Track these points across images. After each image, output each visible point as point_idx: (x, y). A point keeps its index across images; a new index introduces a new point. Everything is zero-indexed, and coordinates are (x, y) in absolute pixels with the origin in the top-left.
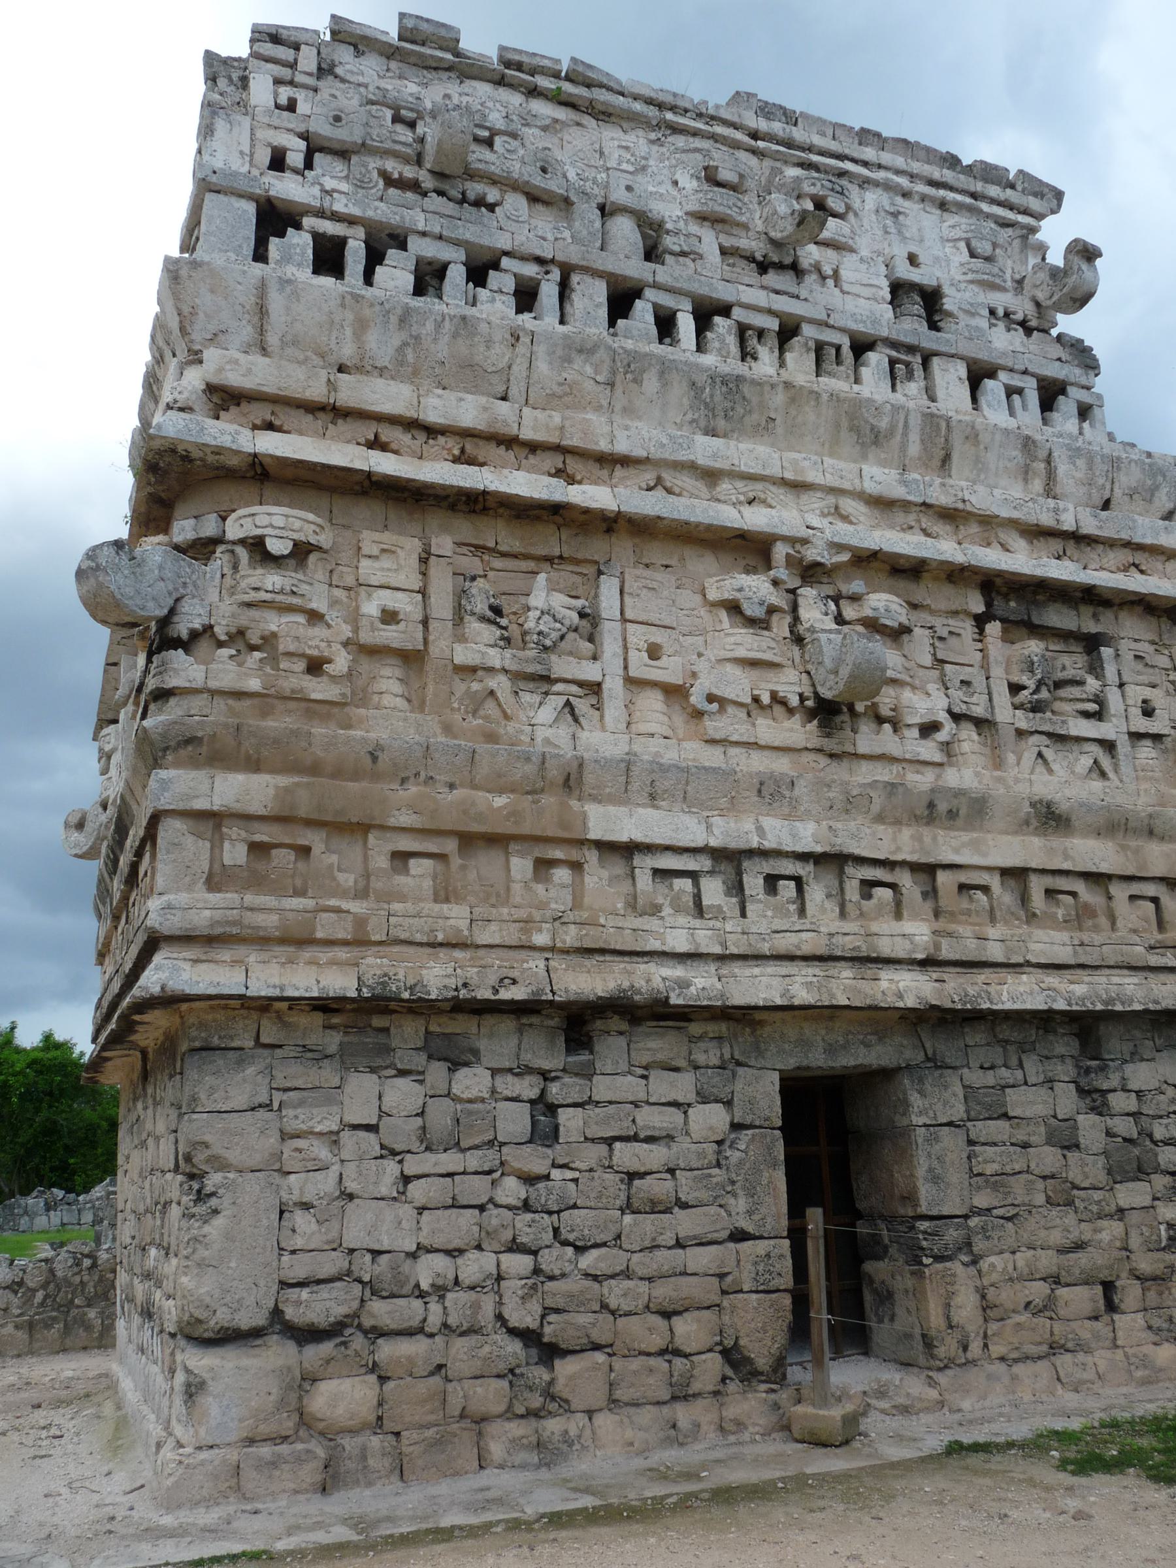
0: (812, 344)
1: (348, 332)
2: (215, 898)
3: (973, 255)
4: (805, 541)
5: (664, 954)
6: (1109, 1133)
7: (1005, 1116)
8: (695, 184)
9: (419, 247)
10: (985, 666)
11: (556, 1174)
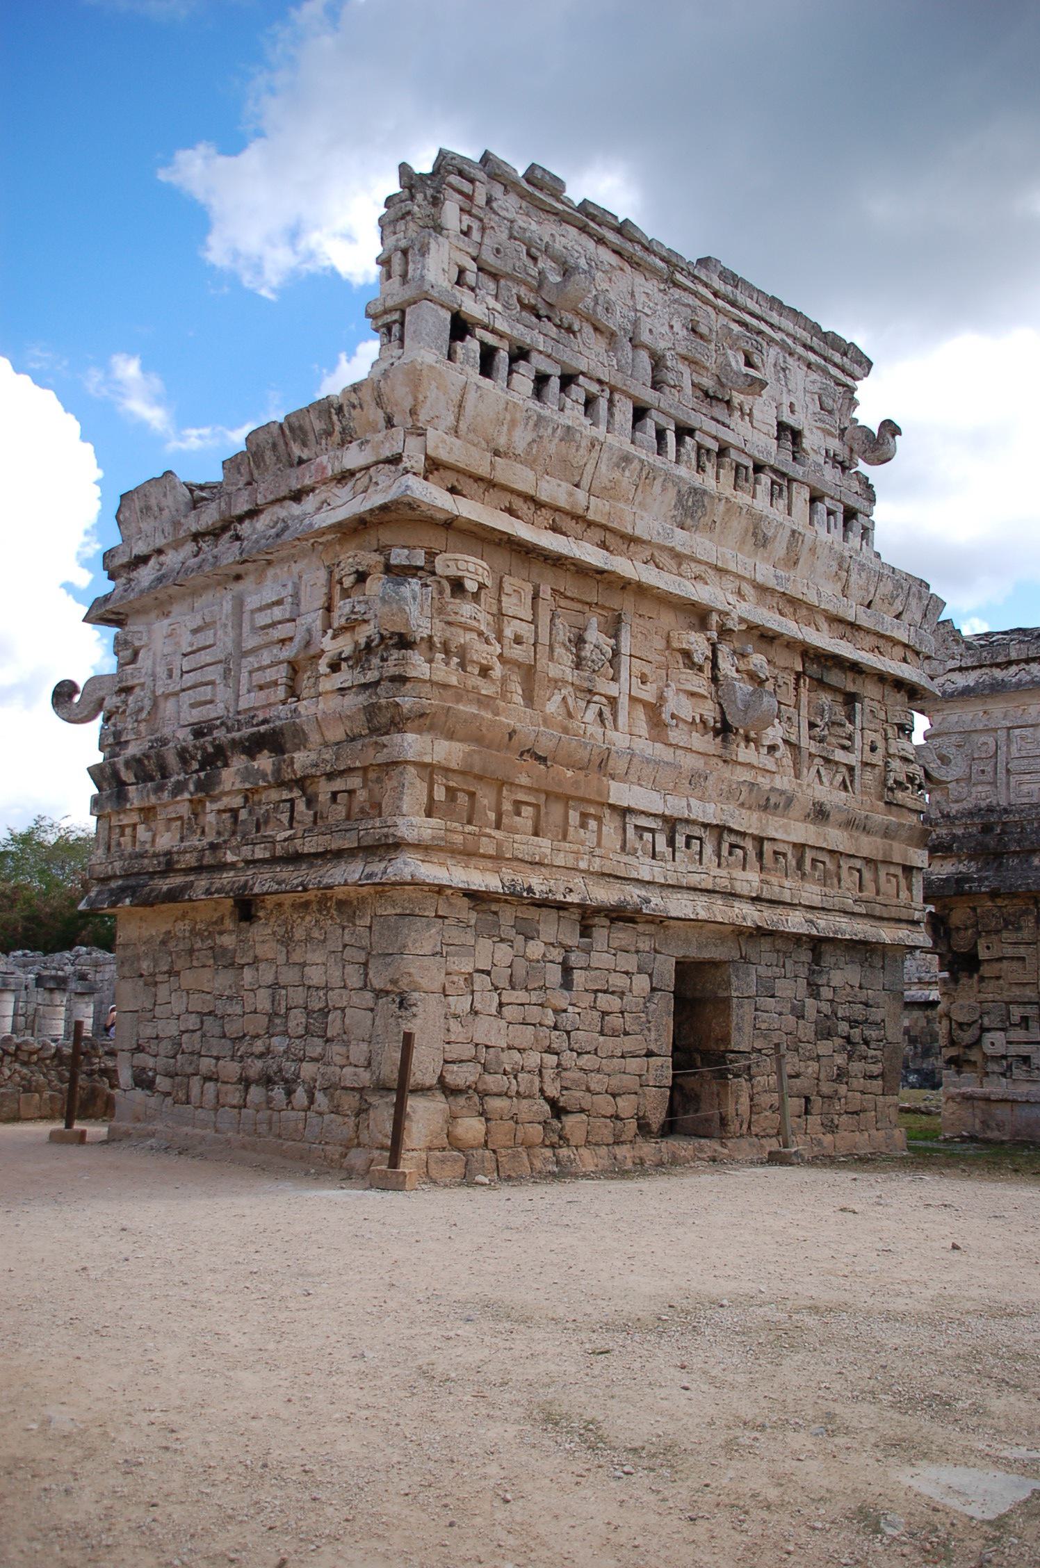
1: (505, 428)
2: (433, 821)
4: (727, 614)
5: (637, 880)
7: (773, 996)
8: (685, 331)
9: (539, 363)
10: (797, 706)
11: (570, 1009)
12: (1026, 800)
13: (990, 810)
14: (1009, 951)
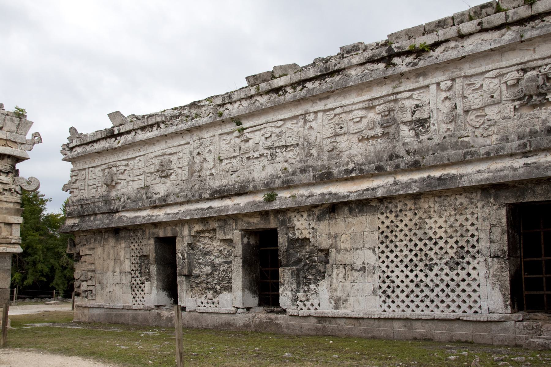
12: (92, 195)
13: (83, 200)
14: (88, 252)
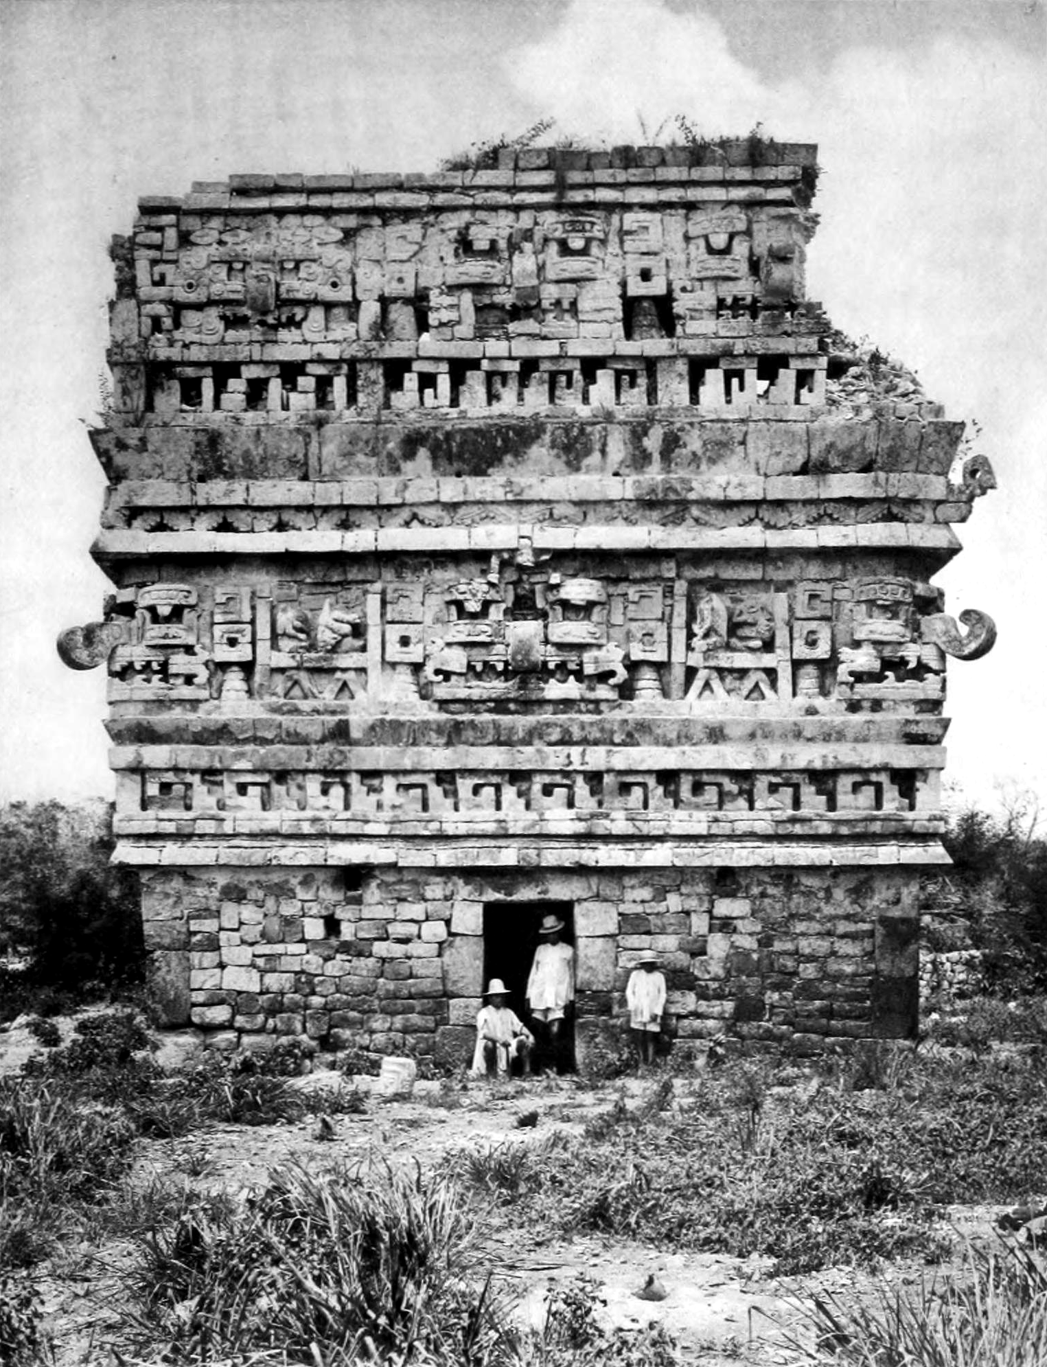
0: (546, 376)
3: (711, 250)
6: (732, 945)
